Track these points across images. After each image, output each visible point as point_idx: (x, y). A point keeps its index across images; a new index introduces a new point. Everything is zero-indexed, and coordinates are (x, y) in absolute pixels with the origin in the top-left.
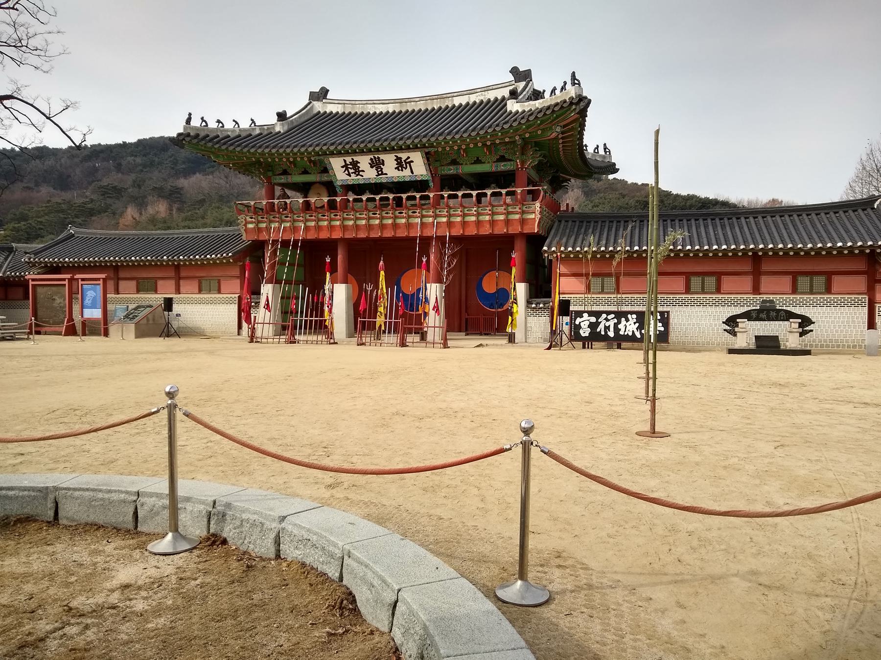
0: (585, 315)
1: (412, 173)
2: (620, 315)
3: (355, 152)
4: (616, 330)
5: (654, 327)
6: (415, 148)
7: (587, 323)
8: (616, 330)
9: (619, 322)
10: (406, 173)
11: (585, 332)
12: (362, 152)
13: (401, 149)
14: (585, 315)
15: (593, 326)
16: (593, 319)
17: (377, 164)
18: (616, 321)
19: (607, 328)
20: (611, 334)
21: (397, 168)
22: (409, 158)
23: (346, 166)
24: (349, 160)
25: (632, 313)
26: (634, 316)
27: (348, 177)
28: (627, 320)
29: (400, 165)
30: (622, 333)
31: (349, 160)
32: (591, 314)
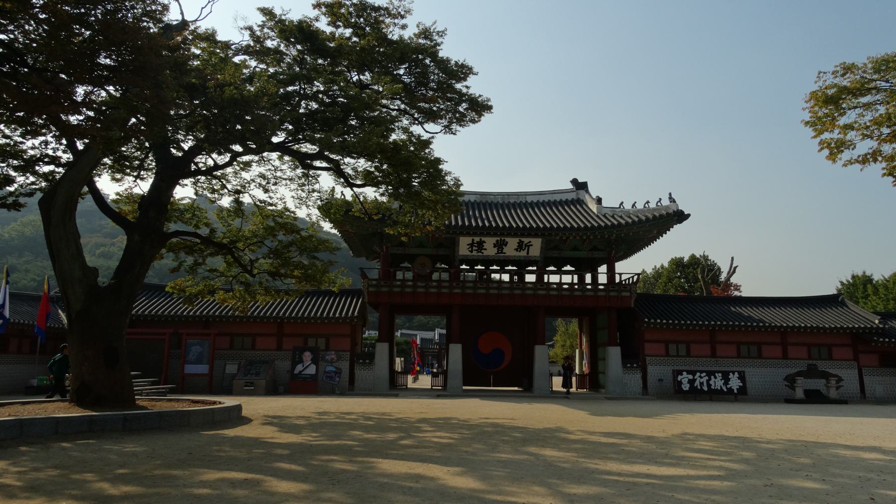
0: (684, 373)
1: (528, 253)
2: (710, 374)
3: (482, 234)
4: (709, 385)
5: (735, 383)
6: (536, 236)
7: (687, 380)
8: (709, 385)
9: (710, 379)
10: (523, 253)
11: (686, 387)
12: (488, 235)
13: (523, 235)
14: (684, 373)
15: (692, 382)
16: (691, 377)
17: (500, 245)
18: (707, 378)
19: (701, 384)
20: (705, 388)
21: (516, 250)
23: (471, 245)
24: (477, 239)
25: (718, 372)
27: (469, 253)
28: (716, 378)
29: (520, 247)
30: (713, 387)
31: (477, 239)
32: (689, 372)
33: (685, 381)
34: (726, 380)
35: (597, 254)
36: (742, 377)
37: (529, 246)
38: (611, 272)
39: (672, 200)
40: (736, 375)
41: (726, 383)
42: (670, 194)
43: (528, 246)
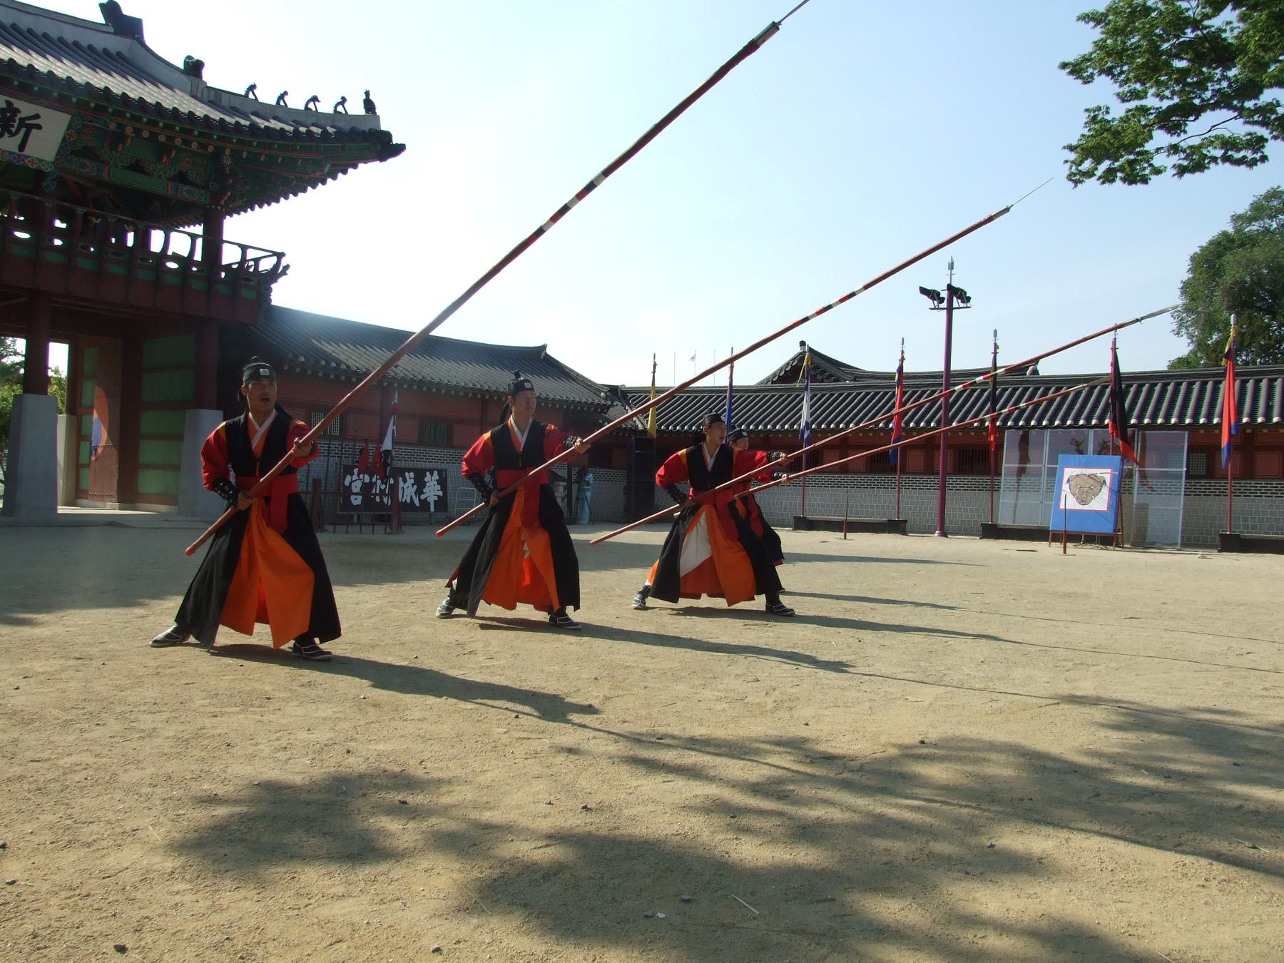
1: (22, 147)
5: (432, 491)
22: (37, 116)
25: (409, 470)
26: (412, 475)
28: (405, 481)
33: (356, 487)
34: (420, 485)
35: (185, 193)
36: (442, 482)
37: (30, 128)
38: (213, 242)
39: (369, 105)
40: (436, 476)
41: (419, 492)
42: (367, 93)
43: (29, 126)
